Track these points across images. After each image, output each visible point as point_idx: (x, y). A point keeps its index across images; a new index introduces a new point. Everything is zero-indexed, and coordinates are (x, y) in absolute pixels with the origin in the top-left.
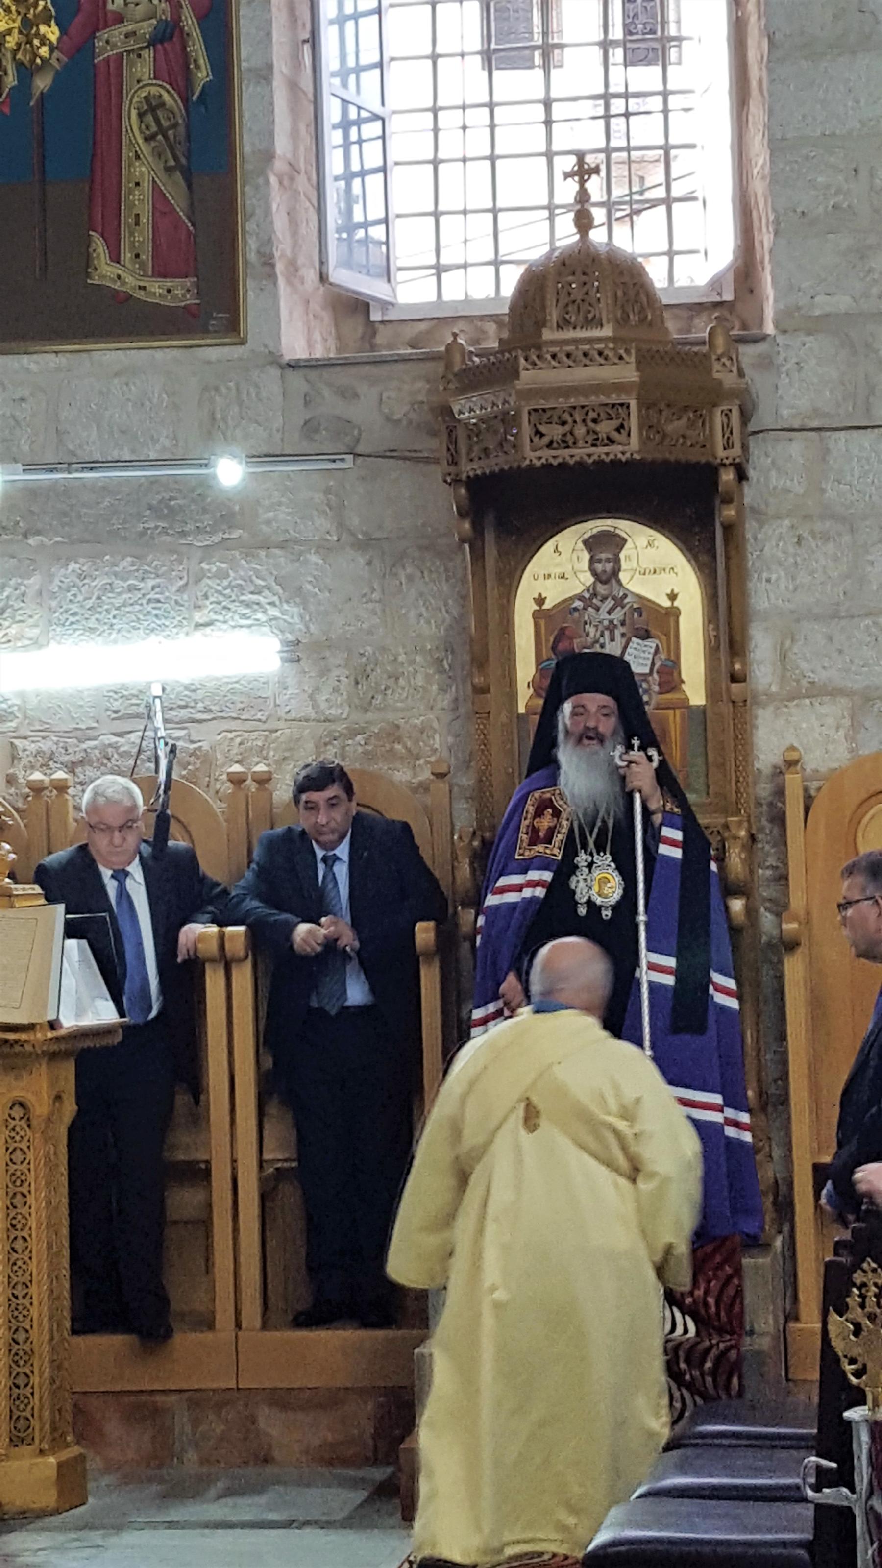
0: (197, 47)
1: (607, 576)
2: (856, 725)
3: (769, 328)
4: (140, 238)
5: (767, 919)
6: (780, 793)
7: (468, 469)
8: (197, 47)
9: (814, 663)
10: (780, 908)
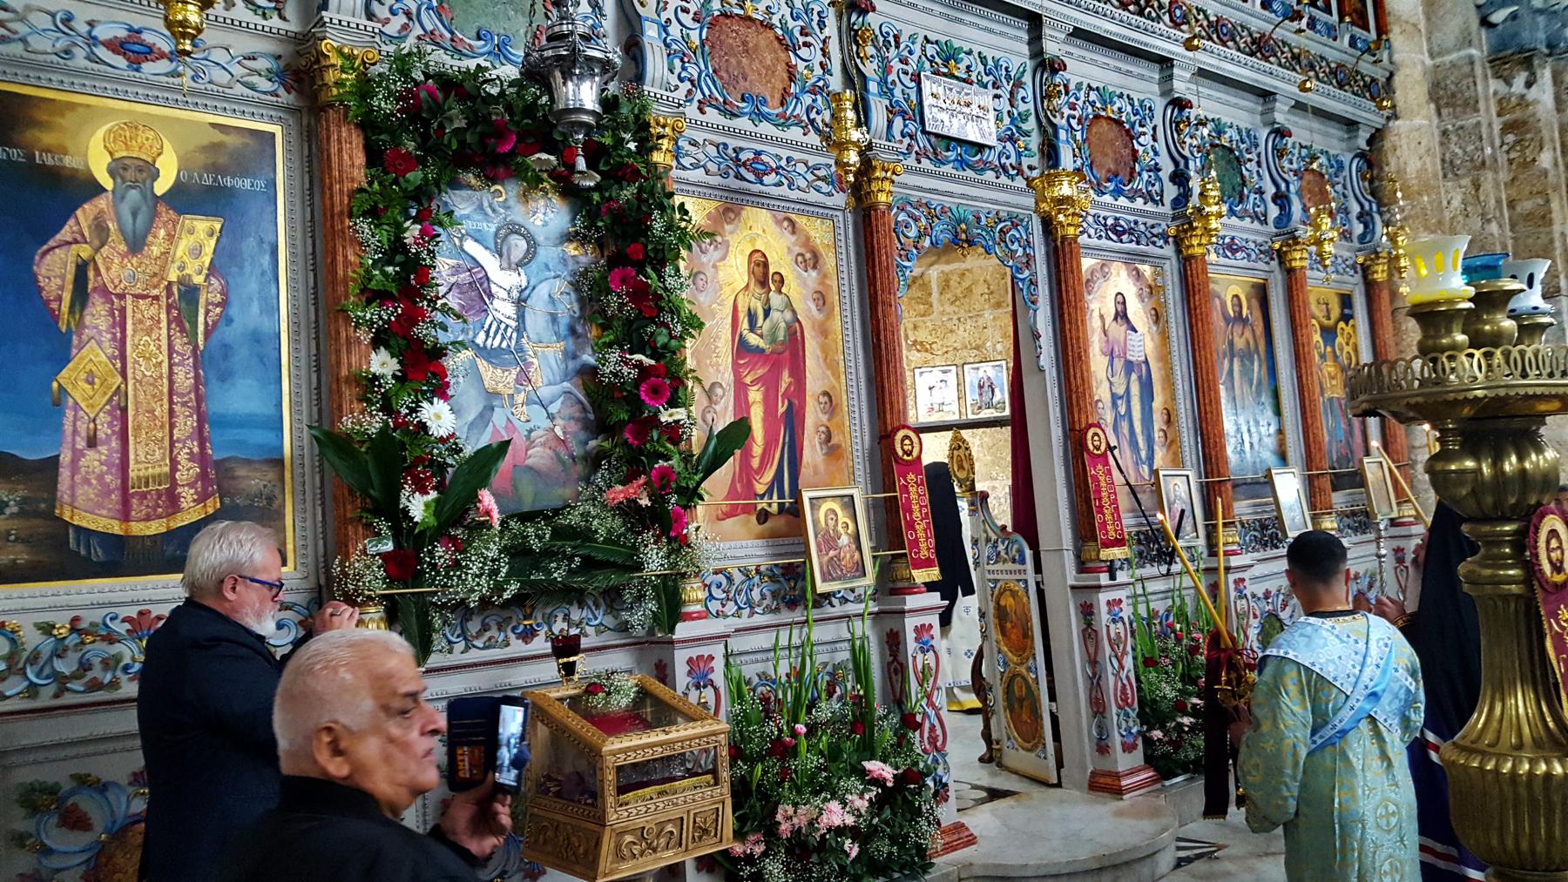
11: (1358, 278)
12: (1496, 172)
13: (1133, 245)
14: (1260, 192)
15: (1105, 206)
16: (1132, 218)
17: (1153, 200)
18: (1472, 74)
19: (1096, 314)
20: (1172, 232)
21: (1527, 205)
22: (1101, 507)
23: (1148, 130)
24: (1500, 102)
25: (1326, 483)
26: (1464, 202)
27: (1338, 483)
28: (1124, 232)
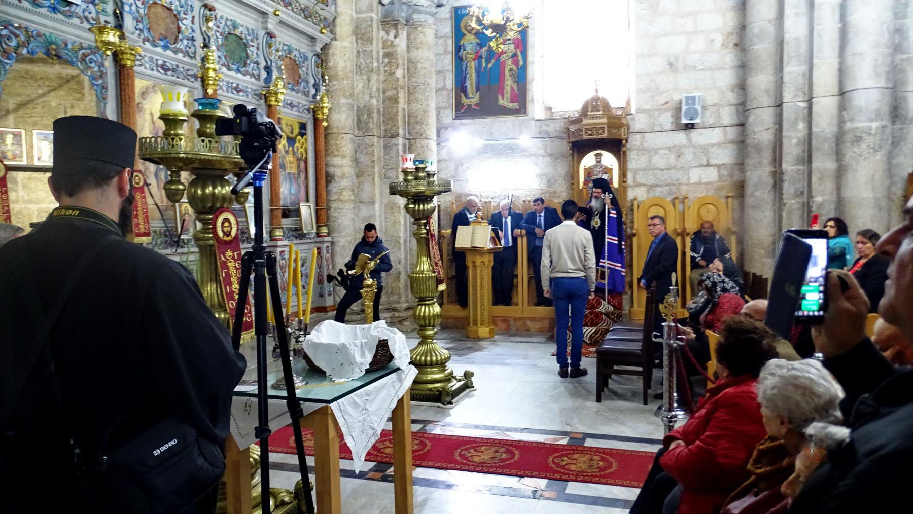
0: (520, 58)
1: (599, 162)
2: (648, 192)
3: (633, 112)
4: (508, 95)
5: (629, 230)
6: (632, 205)
7: (572, 140)
8: (520, 58)
9: (641, 178)
10: (632, 228)
11: (311, 116)
12: (379, 75)
13: (174, 78)
14: (257, 63)
15: (156, 53)
16: (175, 63)
17: (189, 55)
18: (371, 26)
19: (148, 112)
20: (200, 75)
21: (390, 93)
22: (137, 215)
23: (189, 17)
24: (384, 42)
25: (279, 213)
26: (363, 87)
27: (286, 214)
28: (169, 70)
